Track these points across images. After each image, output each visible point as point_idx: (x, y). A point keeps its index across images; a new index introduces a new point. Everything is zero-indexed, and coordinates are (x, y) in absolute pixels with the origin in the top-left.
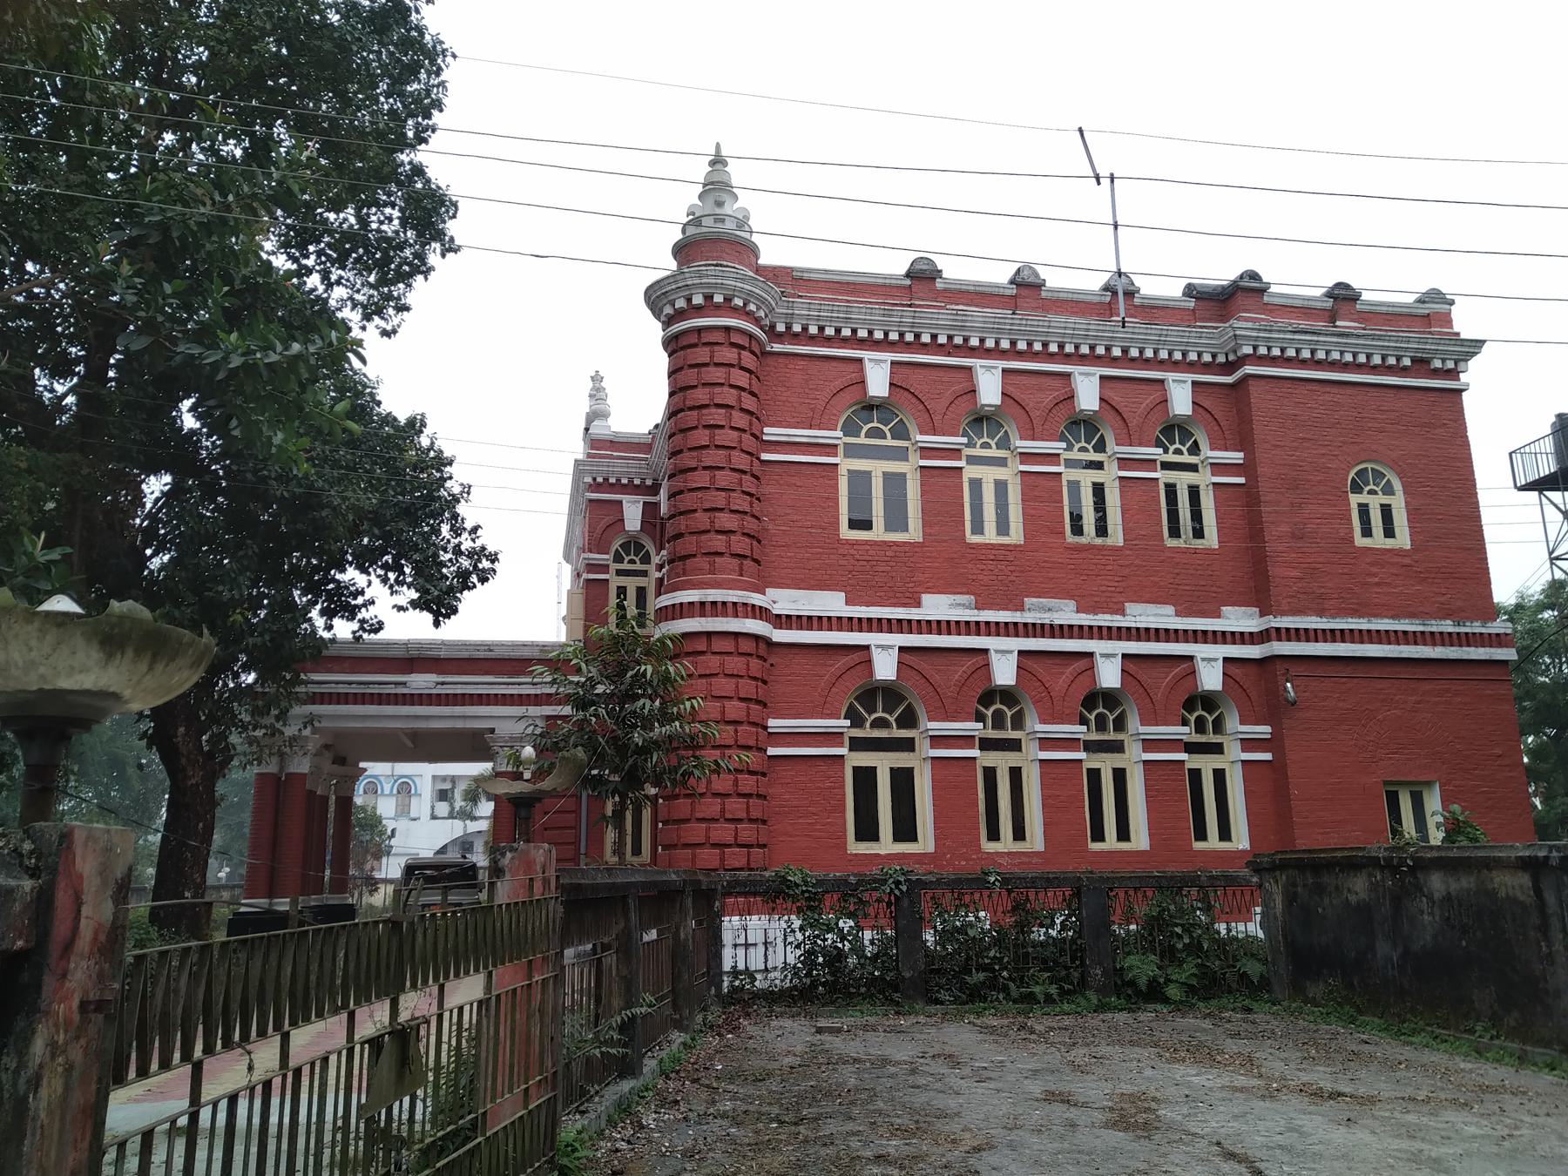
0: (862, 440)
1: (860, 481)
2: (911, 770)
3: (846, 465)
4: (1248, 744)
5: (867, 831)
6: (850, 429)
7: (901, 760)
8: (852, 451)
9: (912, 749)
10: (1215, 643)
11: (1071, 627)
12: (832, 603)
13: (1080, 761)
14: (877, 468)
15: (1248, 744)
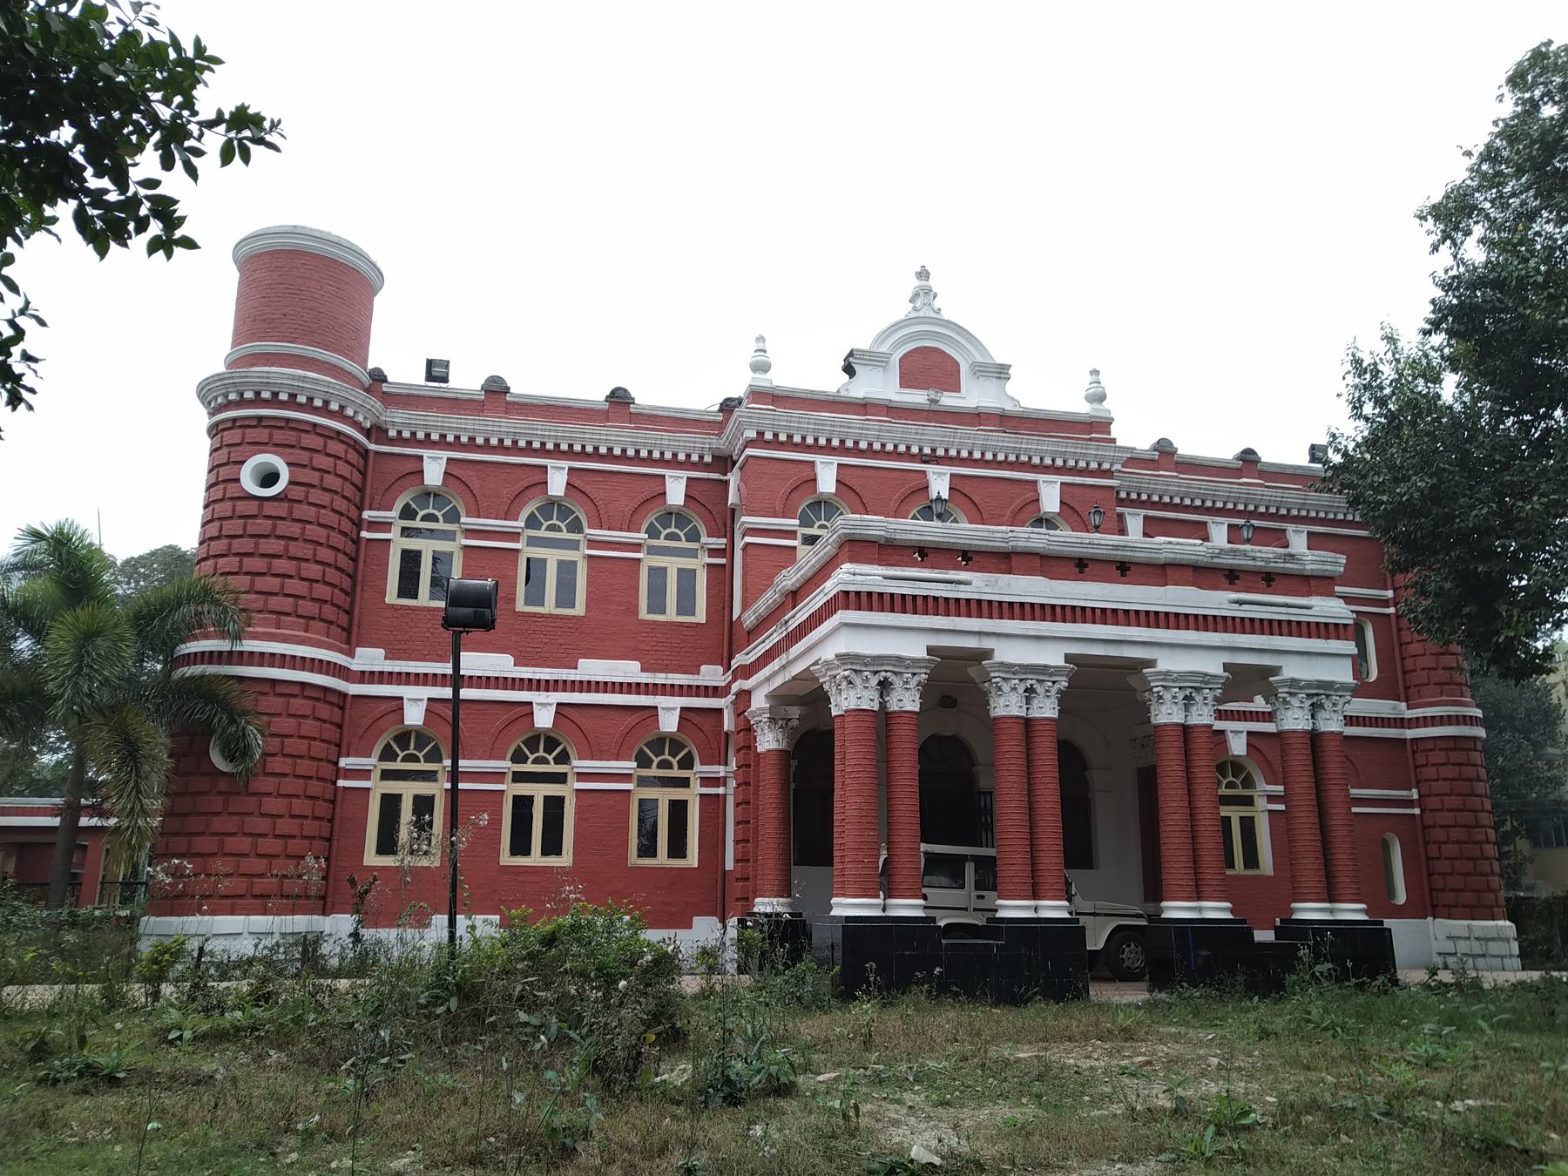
0: (662, 542)
1: (658, 574)
2: (686, 802)
3: (649, 561)
4: (1272, 798)
5: (648, 850)
6: (653, 533)
7: (678, 794)
8: (653, 551)
9: (688, 786)
10: (673, 695)
11: (638, 684)
12: (628, 670)
13: (629, 791)
14: (673, 565)
15: (1272, 798)
